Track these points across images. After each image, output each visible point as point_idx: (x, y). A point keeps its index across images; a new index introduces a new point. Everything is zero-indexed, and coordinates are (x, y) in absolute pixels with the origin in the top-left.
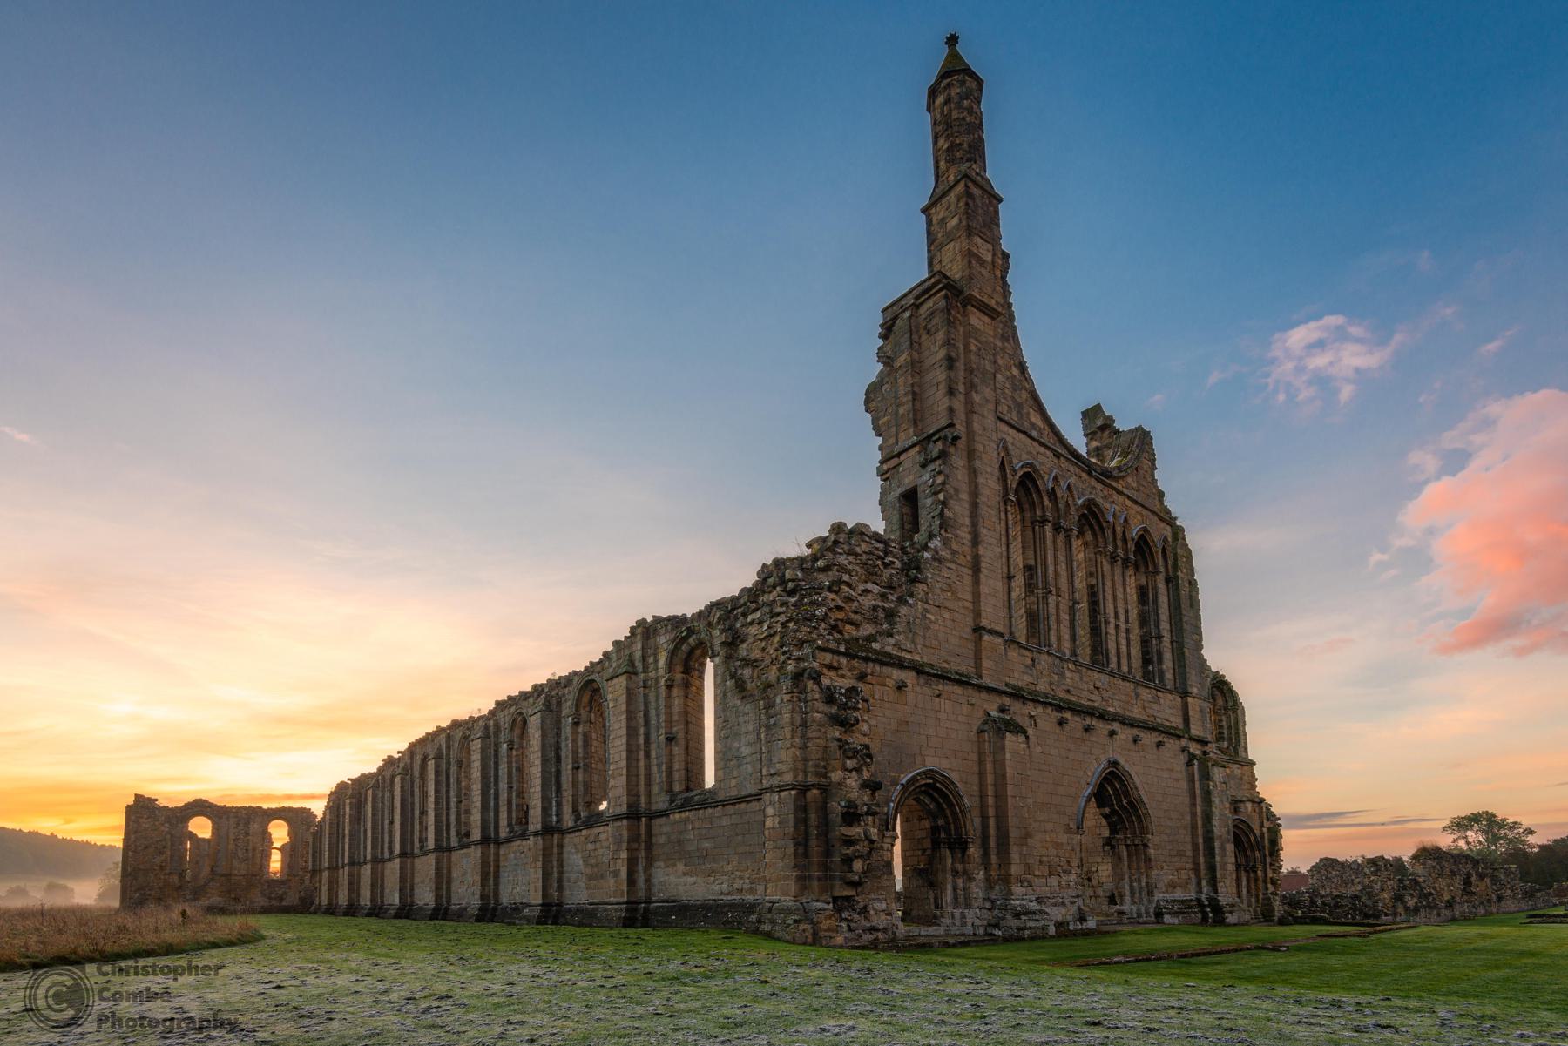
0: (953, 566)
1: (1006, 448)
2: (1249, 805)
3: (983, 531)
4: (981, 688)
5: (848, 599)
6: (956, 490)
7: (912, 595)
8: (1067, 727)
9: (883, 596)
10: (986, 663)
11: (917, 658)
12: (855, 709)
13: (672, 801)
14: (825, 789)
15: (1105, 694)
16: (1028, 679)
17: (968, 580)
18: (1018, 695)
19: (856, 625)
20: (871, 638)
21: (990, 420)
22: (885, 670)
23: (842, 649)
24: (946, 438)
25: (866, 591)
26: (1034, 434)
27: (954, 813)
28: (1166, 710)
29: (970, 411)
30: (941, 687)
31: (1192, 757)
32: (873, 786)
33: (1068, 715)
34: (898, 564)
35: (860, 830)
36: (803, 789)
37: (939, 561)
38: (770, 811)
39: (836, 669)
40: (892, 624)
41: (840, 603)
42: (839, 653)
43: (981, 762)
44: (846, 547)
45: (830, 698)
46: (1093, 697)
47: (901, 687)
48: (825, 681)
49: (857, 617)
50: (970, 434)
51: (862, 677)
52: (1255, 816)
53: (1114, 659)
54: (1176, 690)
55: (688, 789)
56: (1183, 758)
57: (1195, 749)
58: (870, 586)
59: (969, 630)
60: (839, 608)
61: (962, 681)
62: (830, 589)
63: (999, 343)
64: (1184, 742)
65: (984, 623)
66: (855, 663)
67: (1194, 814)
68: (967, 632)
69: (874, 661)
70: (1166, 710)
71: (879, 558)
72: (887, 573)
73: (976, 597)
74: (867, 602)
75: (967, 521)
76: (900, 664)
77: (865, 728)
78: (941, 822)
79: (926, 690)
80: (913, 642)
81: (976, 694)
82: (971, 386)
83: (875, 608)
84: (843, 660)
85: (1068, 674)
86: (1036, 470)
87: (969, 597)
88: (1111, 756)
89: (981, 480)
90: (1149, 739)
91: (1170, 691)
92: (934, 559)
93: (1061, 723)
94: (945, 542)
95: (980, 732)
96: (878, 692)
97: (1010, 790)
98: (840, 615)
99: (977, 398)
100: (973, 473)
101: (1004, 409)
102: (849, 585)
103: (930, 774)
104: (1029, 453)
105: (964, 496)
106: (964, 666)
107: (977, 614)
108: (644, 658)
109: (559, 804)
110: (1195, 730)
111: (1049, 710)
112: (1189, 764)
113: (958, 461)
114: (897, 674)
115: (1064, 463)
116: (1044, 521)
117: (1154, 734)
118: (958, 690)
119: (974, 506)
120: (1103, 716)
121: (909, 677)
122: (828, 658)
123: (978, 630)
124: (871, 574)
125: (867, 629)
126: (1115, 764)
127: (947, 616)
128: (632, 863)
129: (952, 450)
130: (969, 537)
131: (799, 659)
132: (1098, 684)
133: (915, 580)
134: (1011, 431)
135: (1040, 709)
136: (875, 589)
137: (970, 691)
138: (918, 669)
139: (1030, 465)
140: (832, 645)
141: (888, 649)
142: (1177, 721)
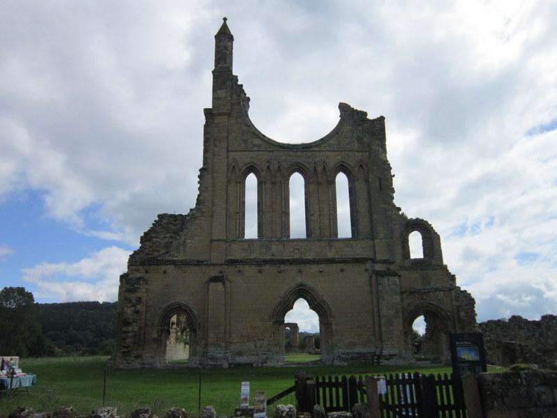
0: (203, 218)
5: (154, 243)
7: (179, 235)
18: (232, 263)
19: (158, 251)
26: (256, 148)
33: (267, 267)
37: (195, 218)
47: (165, 272)
49: (158, 249)
51: (147, 272)
61: (199, 263)
64: (368, 265)
65: (214, 237)
70: (361, 250)
74: (165, 241)
84: (141, 267)
85: (274, 247)
86: (255, 164)
88: (299, 280)
90: (334, 268)
91: (363, 239)
100: (213, 178)
104: (252, 157)
110: (379, 257)
111: (253, 266)
112: (371, 277)
114: (163, 268)
121: (170, 269)
126: (302, 285)
127: (197, 239)
134: (239, 153)
138: (174, 263)
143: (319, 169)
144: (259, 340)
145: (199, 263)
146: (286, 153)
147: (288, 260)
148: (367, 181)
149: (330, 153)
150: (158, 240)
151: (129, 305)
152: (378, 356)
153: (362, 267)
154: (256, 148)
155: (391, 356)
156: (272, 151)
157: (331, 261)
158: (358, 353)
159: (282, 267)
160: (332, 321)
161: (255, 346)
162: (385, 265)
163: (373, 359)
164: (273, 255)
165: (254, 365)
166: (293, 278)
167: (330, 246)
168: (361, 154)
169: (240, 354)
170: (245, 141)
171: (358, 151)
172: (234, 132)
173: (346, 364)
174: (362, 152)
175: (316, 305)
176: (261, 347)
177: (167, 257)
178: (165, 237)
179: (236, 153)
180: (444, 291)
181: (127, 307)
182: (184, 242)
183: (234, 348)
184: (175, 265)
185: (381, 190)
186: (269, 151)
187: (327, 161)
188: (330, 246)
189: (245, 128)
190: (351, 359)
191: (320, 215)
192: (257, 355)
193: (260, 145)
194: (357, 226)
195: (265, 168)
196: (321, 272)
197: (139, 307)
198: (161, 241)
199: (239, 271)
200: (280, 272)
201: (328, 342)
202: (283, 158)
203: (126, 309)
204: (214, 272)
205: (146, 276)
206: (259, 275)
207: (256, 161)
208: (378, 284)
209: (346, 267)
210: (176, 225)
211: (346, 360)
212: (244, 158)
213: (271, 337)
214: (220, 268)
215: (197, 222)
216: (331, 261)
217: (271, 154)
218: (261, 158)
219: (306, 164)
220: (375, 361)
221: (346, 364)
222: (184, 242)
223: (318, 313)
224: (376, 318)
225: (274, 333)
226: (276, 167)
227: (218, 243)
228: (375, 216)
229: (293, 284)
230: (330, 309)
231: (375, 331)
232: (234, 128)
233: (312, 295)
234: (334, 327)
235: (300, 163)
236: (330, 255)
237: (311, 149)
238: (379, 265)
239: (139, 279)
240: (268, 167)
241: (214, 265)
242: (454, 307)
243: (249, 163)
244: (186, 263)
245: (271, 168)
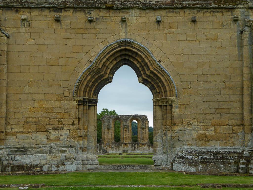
8: (66, 24)
33: (69, 13)
88: (122, 36)
111: (46, 12)
117: (187, 12)
126: (126, 43)
135: (35, 13)
144: (54, 129)
152: (246, 158)
158: (214, 153)
159: (94, 14)
160: (172, 101)
161: (48, 138)
163: (237, 163)
165: (45, 169)
169: (22, 150)
173: (193, 169)
175: (149, 76)
176: (58, 139)
183: (12, 141)
190: (202, 163)
192: (51, 152)
196: (159, 22)
200: (91, 21)
201: (165, 135)
206: (55, 25)
209: (199, 15)
211: (194, 163)
213: (73, 124)
220: (242, 166)
221: (193, 169)
223: (152, 89)
225: (79, 119)
229: (112, 41)
230: (170, 82)
231: (243, 119)
233: (143, 60)
234: (175, 110)
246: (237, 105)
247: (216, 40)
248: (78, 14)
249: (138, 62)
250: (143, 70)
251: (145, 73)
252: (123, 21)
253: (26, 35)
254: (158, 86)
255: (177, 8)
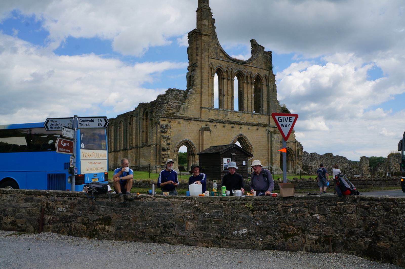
0: (196, 94)
1: (212, 64)
2: (292, 143)
3: (203, 85)
4: (200, 121)
5: (170, 105)
6: (197, 77)
7: (184, 103)
8: (226, 128)
9: (178, 103)
10: (202, 115)
11: (185, 116)
12: (167, 129)
13: (143, 145)
14: (160, 145)
15: (241, 118)
16: (216, 117)
17: (199, 97)
18: (211, 121)
19: (172, 110)
20: (174, 113)
21: (207, 59)
22: (176, 120)
23: (165, 117)
24: (195, 66)
25: (175, 102)
26: (221, 59)
27: (192, 148)
28: (263, 119)
29: (201, 59)
30: (190, 122)
31: (269, 131)
32: (169, 144)
33: (227, 125)
34: (183, 95)
35: (166, 153)
36: (156, 145)
37: (192, 94)
38: (152, 149)
39: (165, 121)
40: (179, 109)
41: (168, 106)
42: (165, 118)
43: (199, 137)
44: (171, 94)
45: (161, 127)
46: (237, 119)
47: (179, 123)
48: (161, 123)
49: (172, 109)
50: (201, 64)
51: (170, 122)
52: (294, 146)
53: (246, 108)
54: (267, 115)
55: (146, 142)
56: (266, 132)
57: (271, 129)
58: (176, 101)
59: (199, 108)
60: (168, 107)
61: (196, 120)
62: (166, 104)
63: (211, 41)
64: (267, 128)
65: (203, 106)
66: (169, 119)
67: (268, 146)
68: (199, 108)
69: (173, 118)
70: (263, 119)
71: (178, 95)
72: (180, 98)
73: (201, 100)
74: (174, 105)
75: (200, 83)
76: (179, 118)
77: (170, 132)
78: (190, 150)
79: (186, 123)
80: (184, 112)
81: (200, 122)
82: (202, 53)
83: (176, 106)
84: (166, 119)
85: (229, 114)
86: (221, 67)
87: (200, 100)
88: (240, 133)
89: (203, 74)
90: (254, 128)
91: (265, 115)
92: (190, 93)
93: (224, 127)
94: (194, 89)
95: (200, 131)
96: (174, 124)
97: (204, 143)
98: (168, 108)
99: (203, 56)
100: (202, 72)
101: (212, 55)
102: (170, 102)
103: (186, 140)
104: (220, 64)
105: (199, 78)
106: (197, 116)
107: (201, 104)
108: (139, 113)
109: (127, 144)
112: (268, 134)
113: (198, 70)
114: (178, 120)
115: (230, 63)
116: (224, 79)
118: (194, 122)
119: (201, 80)
120: (237, 123)
121: (182, 121)
122: (163, 119)
123: (201, 108)
124: (176, 99)
125: (175, 111)
126: (241, 135)
127: (193, 105)
128: (136, 158)
129: (197, 68)
130: (200, 87)
131: (157, 119)
132: (239, 116)
133: (185, 99)
134: (214, 60)
135: (218, 124)
136: (177, 101)
137: (198, 122)
138: (184, 118)
139: (220, 66)
140: (163, 116)
141: (178, 115)
142: (266, 122)
143: (249, 76)
145: (196, 120)
146: (235, 64)
147: (236, 122)
148: (267, 86)
149: (253, 68)
150: (171, 103)
151: (164, 140)
153: (265, 129)
154: (221, 59)
155: (276, 170)
156: (229, 62)
157: (252, 124)
159: (233, 125)
162: (273, 128)
164: (229, 118)
166: (237, 131)
167: (252, 117)
168: (265, 71)
170: (217, 53)
171: (265, 70)
172: (211, 47)
174: (266, 70)
175: (245, 145)
177: (178, 114)
178: (175, 102)
179: (212, 60)
180: (293, 142)
181: (163, 141)
182: (187, 106)
184: (184, 119)
185: (273, 91)
186: (227, 62)
187: (252, 72)
188: (252, 117)
189: (216, 46)
191: (248, 100)
193: (223, 58)
194: (263, 107)
195: (225, 71)
197: (168, 142)
198: (173, 104)
199: (215, 126)
202: (233, 67)
203: (162, 142)
204: (203, 125)
205: (170, 124)
206: (223, 128)
207: (221, 66)
208: (272, 137)
210: (180, 96)
212: (216, 63)
214: (205, 123)
215: (193, 96)
216: (252, 124)
217: (228, 63)
218: (224, 65)
219: (243, 72)
222: (187, 106)
224: (270, 153)
226: (230, 71)
227: (204, 109)
228: (271, 104)
229: (238, 134)
231: (268, 159)
232: (211, 45)
235: (241, 71)
236: (252, 121)
237: (246, 64)
238: (271, 128)
239: (167, 125)
240: (227, 71)
241: (203, 121)
242: (297, 150)
243: (218, 67)
244: (190, 119)
245: (228, 71)
246: (267, 154)
247: (262, 135)
248: (229, 125)
249: (243, 141)
250: (244, 142)
251: (244, 144)
252: (241, 128)
253: (216, 131)
254: (248, 148)
255: (254, 125)
